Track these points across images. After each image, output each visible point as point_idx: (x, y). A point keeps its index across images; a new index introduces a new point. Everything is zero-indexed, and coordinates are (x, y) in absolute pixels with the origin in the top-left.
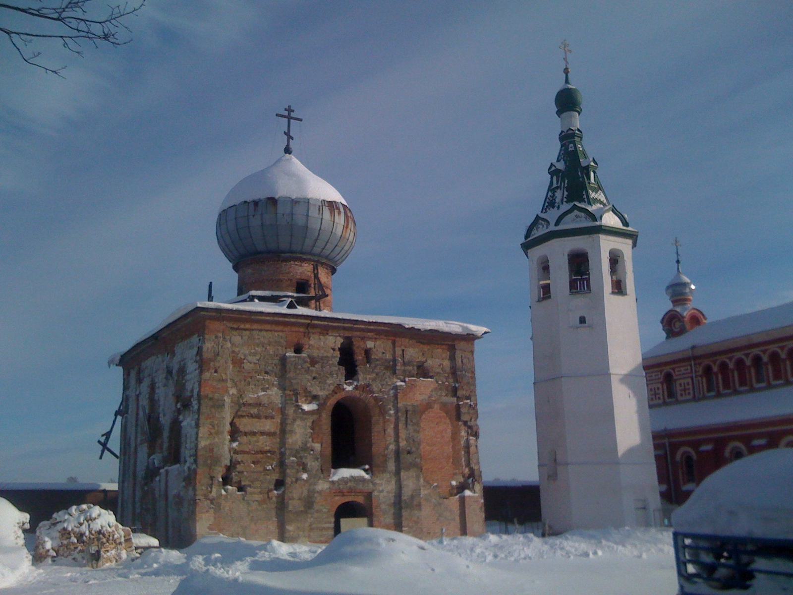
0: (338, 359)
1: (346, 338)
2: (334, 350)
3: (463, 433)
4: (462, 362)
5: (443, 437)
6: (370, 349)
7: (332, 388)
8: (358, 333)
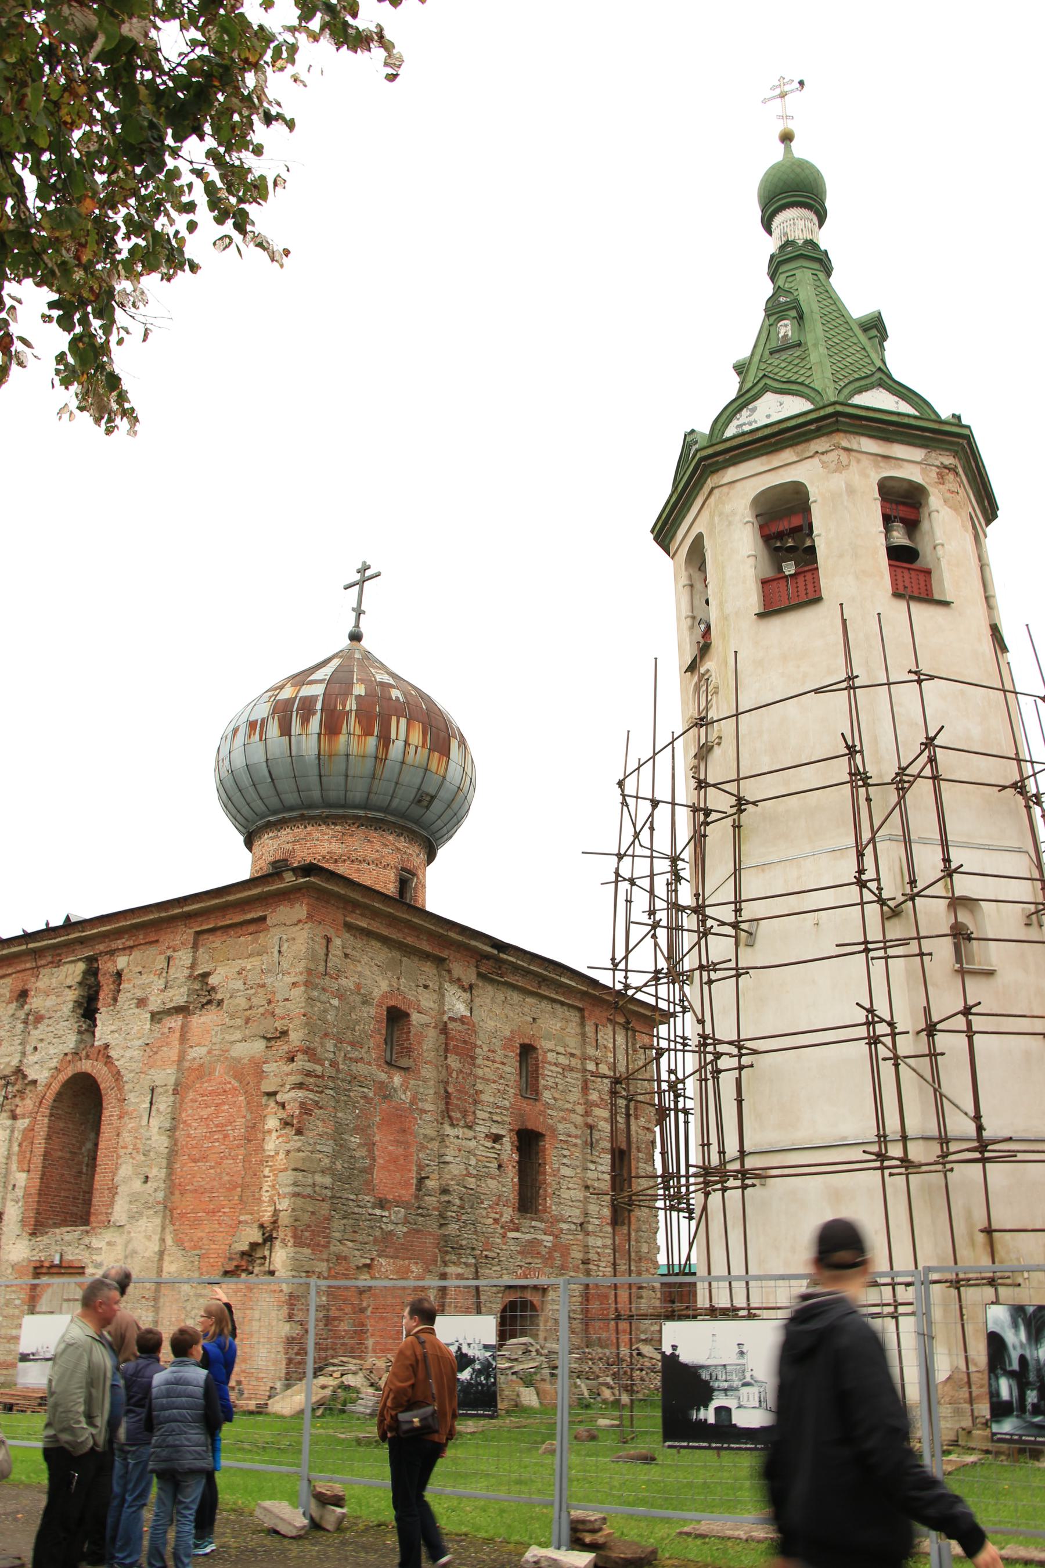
0: (71, 1005)
1: (91, 960)
2: (70, 987)
3: (272, 1123)
4: (280, 952)
5: (226, 1136)
6: (122, 970)
7: (54, 1063)
8: (101, 947)
